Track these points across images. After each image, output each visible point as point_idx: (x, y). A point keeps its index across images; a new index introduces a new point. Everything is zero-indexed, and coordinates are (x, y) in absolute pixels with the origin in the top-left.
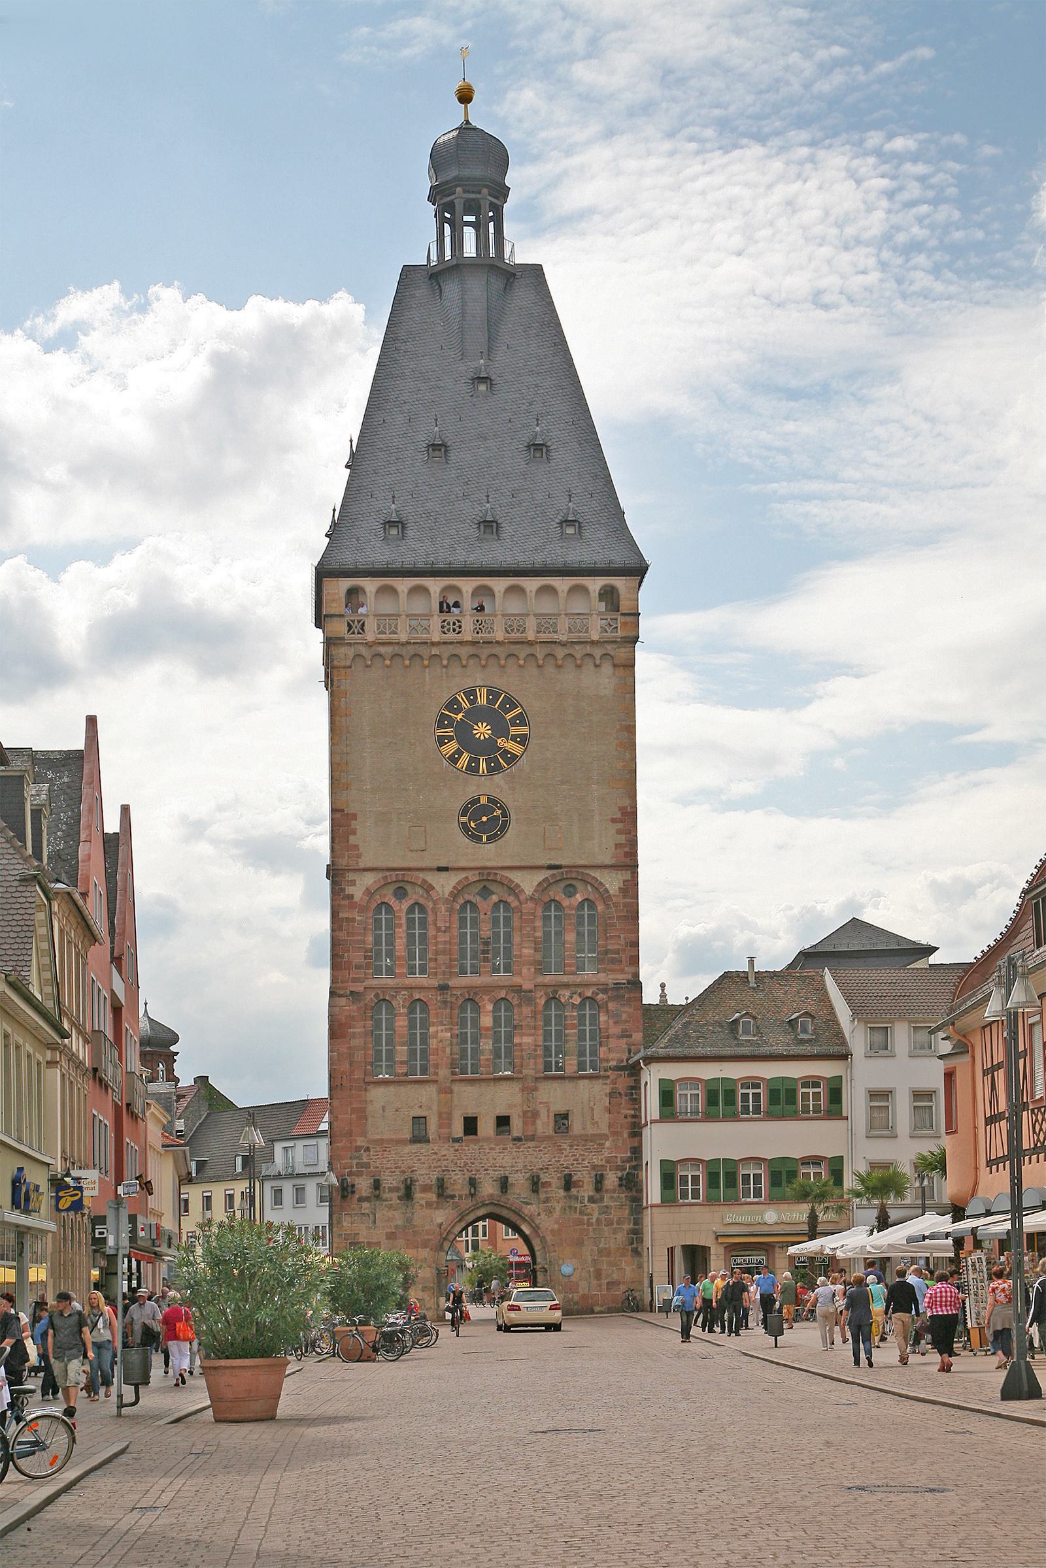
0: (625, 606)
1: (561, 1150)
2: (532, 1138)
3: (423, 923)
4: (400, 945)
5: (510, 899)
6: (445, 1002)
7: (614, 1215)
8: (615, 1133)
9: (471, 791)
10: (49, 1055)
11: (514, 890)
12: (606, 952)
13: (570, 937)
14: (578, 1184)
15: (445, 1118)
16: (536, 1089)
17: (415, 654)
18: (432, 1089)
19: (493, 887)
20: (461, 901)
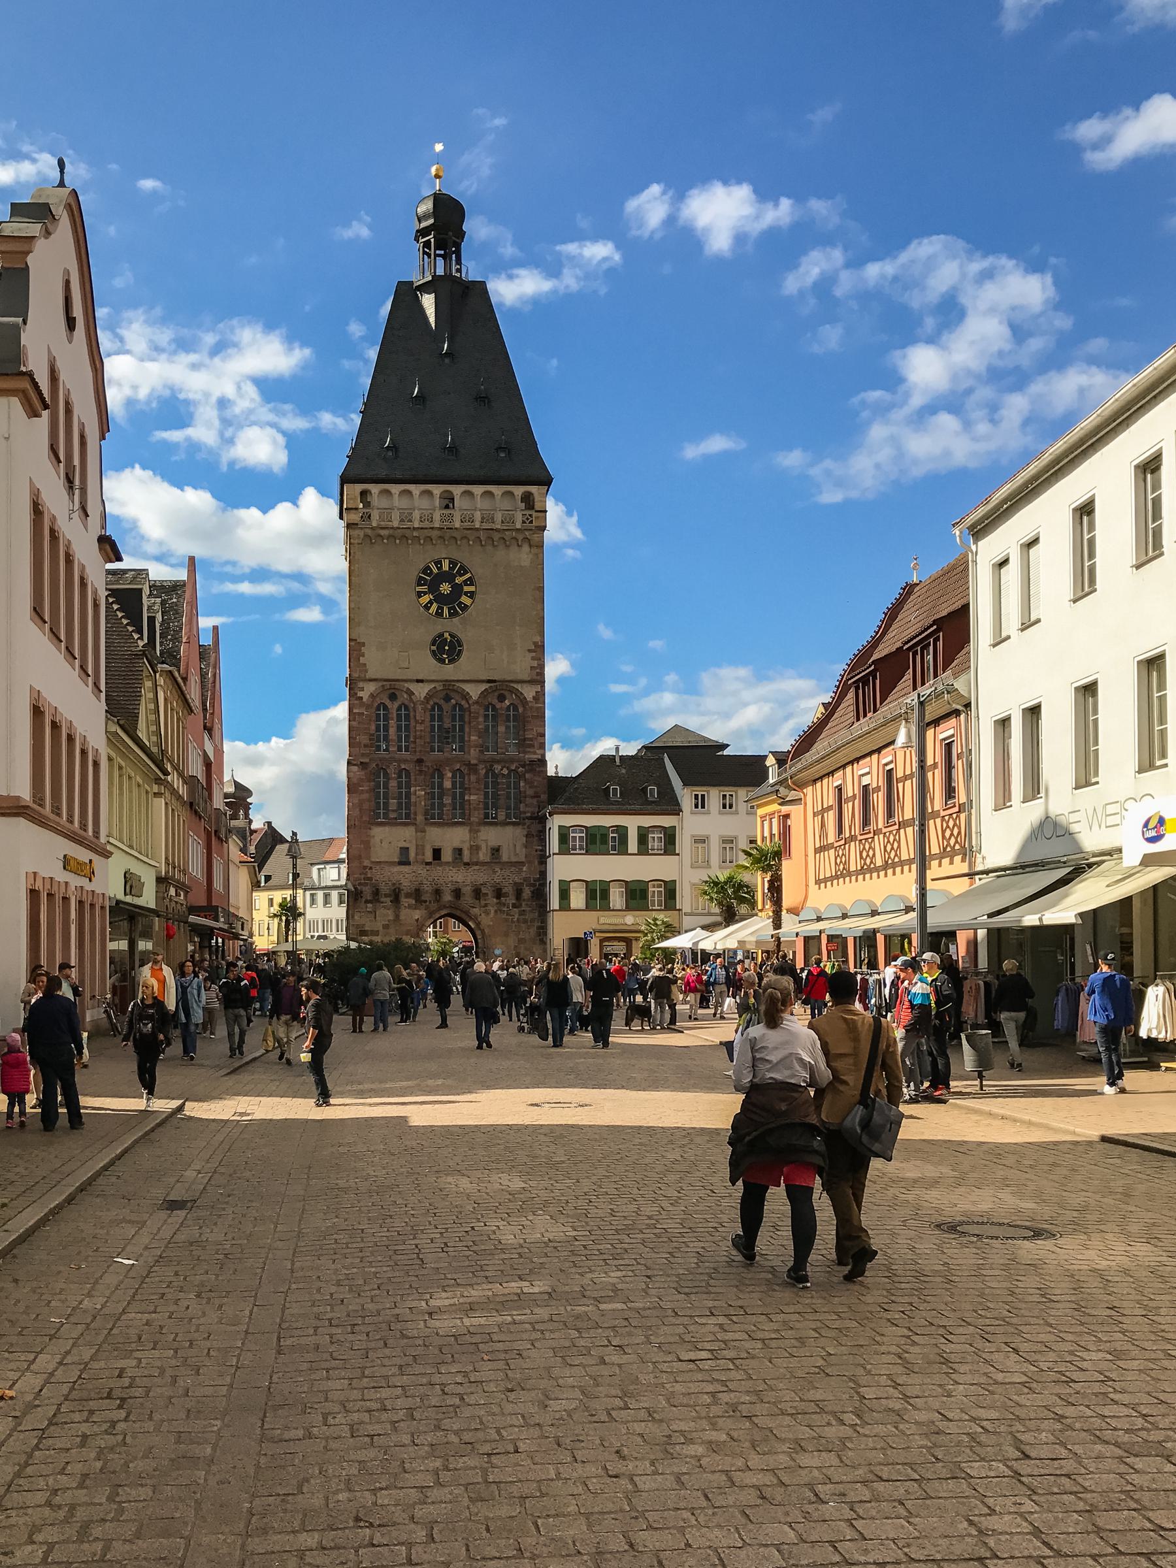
0: (538, 506)
1: (495, 872)
2: (476, 864)
3: (407, 717)
4: (392, 731)
5: (463, 702)
6: (421, 771)
7: (528, 916)
8: (529, 862)
10: (156, 788)
11: (465, 696)
12: (525, 739)
13: (501, 729)
14: (506, 895)
15: (420, 849)
16: (479, 831)
17: (402, 536)
18: (412, 829)
19: (452, 694)
20: (431, 703)
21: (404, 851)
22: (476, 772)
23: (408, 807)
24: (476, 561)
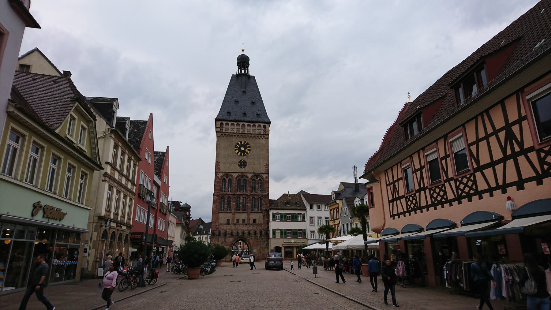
0: (267, 129)
3: (231, 183)
4: (227, 186)
7: (263, 240)
9: (240, 159)
11: (247, 177)
13: (257, 186)
14: (257, 234)
15: (233, 220)
17: (232, 135)
21: (228, 220)
22: (250, 197)
23: (230, 207)
24: (250, 141)
